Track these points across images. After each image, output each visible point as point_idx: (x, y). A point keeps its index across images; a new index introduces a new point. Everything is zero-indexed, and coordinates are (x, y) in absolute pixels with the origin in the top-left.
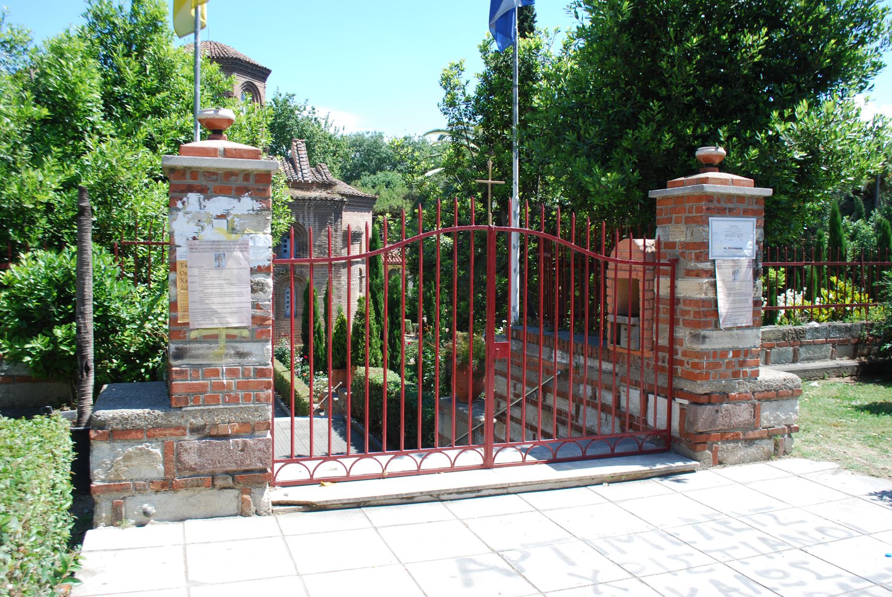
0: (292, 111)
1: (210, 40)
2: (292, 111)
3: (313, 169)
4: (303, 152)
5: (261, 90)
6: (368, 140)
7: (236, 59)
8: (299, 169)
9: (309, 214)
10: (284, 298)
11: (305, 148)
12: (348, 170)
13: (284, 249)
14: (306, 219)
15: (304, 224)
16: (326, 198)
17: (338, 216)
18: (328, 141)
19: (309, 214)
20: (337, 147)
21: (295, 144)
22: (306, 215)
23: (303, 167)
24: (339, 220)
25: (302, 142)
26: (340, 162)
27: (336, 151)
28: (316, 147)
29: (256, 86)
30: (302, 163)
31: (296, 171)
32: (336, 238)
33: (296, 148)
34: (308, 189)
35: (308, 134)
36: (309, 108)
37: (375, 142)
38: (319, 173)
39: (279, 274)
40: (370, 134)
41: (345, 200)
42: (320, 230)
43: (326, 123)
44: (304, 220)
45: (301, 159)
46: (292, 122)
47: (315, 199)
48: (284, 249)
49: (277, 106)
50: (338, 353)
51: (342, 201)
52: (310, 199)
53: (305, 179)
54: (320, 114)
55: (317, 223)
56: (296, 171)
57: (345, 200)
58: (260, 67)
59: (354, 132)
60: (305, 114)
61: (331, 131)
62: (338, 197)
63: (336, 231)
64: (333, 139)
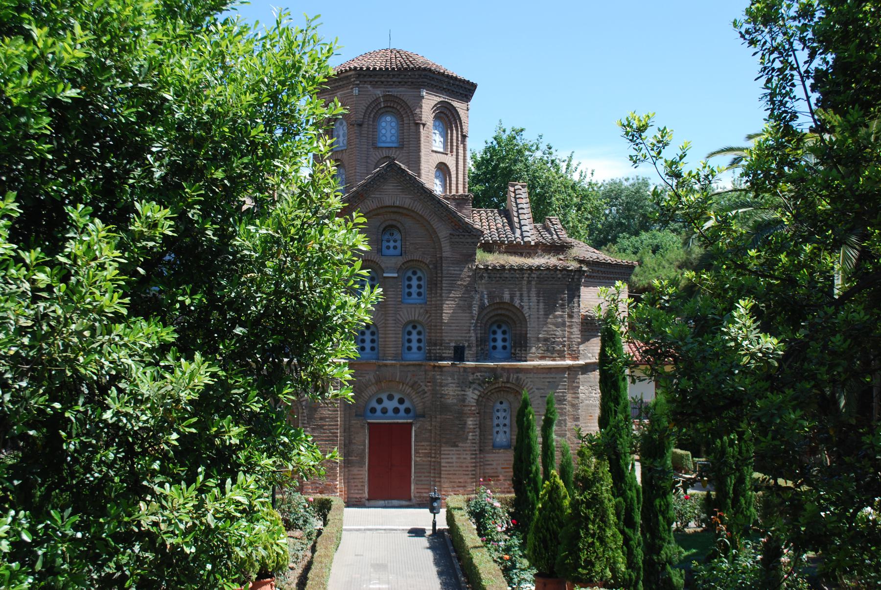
0: (520, 152)
2: (520, 152)
3: (538, 225)
4: (524, 201)
5: (462, 113)
6: (627, 189)
7: (425, 69)
8: (517, 225)
9: (529, 291)
10: (491, 419)
11: (526, 195)
12: (600, 231)
13: (492, 344)
14: (525, 299)
15: (522, 307)
16: (555, 266)
17: (574, 294)
18: (570, 191)
19: (529, 291)
20: (582, 199)
21: (512, 189)
23: (523, 222)
24: (576, 300)
26: (587, 219)
27: (582, 204)
28: (554, 199)
29: (454, 108)
30: (521, 217)
32: (570, 327)
33: (513, 195)
34: (529, 255)
35: (541, 182)
36: (543, 147)
37: (638, 192)
38: (547, 229)
39: (484, 382)
40: (631, 181)
41: (585, 268)
42: (547, 315)
43: (568, 166)
44: (522, 300)
45: (520, 211)
46: (520, 166)
47: (538, 268)
48: (492, 344)
49: (500, 146)
50: (546, 548)
51: (579, 271)
52: (530, 268)
53: (526, 239)
54: (560, 155)
55: (541, 305)
57: (585, 268)
58: (460, 80)
59: (608, 180)
60: (538, 154)
61: (576, 177)
62: (573, 265)
63: (571, 316)
64: (577, 188)
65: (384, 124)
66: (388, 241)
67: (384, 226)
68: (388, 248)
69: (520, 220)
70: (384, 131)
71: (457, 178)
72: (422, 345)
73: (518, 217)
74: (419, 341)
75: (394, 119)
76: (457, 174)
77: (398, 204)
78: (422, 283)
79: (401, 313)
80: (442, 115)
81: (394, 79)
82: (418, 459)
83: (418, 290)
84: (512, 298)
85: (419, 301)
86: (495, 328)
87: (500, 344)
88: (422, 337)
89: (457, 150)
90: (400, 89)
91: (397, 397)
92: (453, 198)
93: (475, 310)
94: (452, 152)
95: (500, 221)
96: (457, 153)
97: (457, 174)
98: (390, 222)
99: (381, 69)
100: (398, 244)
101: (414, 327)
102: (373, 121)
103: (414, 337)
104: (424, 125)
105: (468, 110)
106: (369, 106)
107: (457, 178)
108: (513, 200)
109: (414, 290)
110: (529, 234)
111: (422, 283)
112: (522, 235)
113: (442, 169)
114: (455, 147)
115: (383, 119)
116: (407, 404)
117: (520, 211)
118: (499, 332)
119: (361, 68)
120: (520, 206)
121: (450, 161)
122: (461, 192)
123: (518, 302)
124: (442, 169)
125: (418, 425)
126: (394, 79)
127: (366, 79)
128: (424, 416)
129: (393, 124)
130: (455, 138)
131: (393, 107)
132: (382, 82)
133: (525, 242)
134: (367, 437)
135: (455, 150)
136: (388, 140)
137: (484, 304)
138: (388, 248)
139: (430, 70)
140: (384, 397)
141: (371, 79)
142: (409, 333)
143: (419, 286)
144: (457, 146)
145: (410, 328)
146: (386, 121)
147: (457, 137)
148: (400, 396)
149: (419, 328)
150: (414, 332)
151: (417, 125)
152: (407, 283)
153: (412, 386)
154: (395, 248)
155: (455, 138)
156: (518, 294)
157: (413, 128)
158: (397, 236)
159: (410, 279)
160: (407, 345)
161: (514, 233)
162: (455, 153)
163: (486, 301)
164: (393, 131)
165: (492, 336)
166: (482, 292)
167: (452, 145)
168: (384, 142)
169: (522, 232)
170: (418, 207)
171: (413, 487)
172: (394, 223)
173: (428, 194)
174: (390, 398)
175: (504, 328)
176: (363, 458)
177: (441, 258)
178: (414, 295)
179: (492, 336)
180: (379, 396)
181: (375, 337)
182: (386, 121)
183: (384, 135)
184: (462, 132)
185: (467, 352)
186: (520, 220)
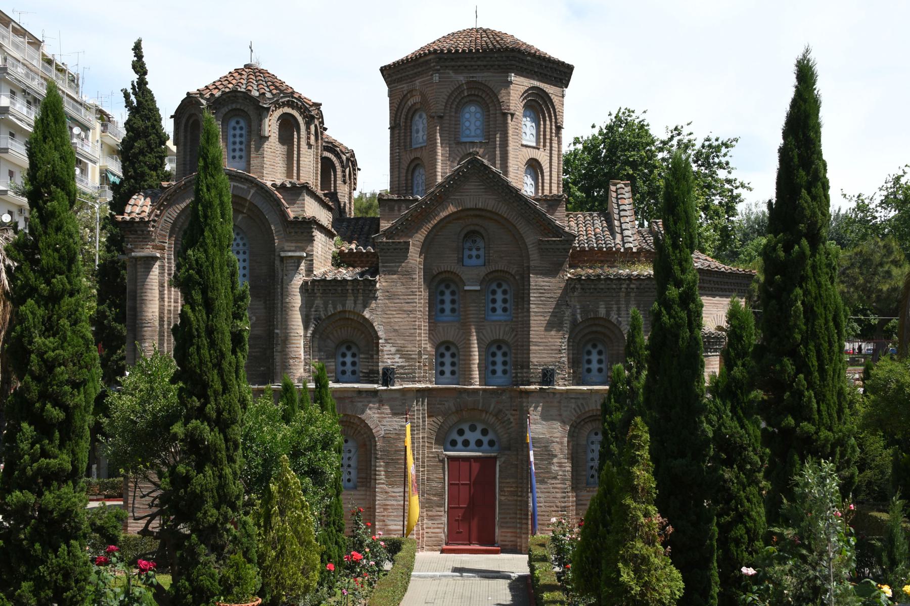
1: (478, 27)
4: (627, 201)
5: (555, 100)
7: (513, 50)
8: (618, 230)
13: (587, 366)
15: (620, 323)
22: (623, 307)
23: (624, 226)
25: (625, 185)
29: (547, 94)
31: (613, 233)
33: (614, 195)
44: (619, 315)
45: (622, 213)
48: (587, 366)
53: (627, 245)
56: (613, 233)
65: (467, 116)
66: (470, 250)
68: (470, 257)
69: (621, 223)
70: (467, 124)
71: (551, 176)
72: (507, 368)
73: (619, 220)
74: (505, 363)
75: (479, 110)
76: (551, 171)
78: (508, 297)
79: (484, 332)
80: (533, 103)
81: (479, 63)
82: (503, 498)
83: (504, 305)
84: (608, 313)
85: (502, 318)
87: (595, 366)
88: (507, 359)
89: (551, 143)
90: (486, 74)
91: (480, 427)
92: (545, 200)
94: (544, 146)
95: (599, 224)
96: (551, 147)
97: (551, 171)
99: (464, 51)
100: (481, 252)
101: (499, 348)
102: (456, 113)
103: (499, 359)
104: (512, 115)
105: (563, 96)
106: (451, 94)
107: (551, 176)
108: (614, 200)
109: (499, 305)
110: (631, 239)
111: (508, 297)
112: (623, 240)
113: (534, 167)
114: (548, 141)
115: (467, 110)
116: (491, 436)
117: (622, 213)
119: (442, 51)
120: (622, 207)
121: (542, 156)
122: (555, 191)
123: (616, 316)
124: (534, 167)
125: (503, 459)
126: (479, 63)
127: (447, 64)
128: (509, 449)
129: (478, 115)
130: (548, 130)
131: (478, 96)
132: (466, 67)
133: (625, 249)
134: (447, 473)
135: (548, 144)
136: (473, 134)
138: (470, 257)
139: (519, 51)
140: (466, 427)
141: (453, 63)
142: (494, 355)
143: (505, 301)
144: (551, 140)
145: (494, 349)
146: (470, 112)
147: (551, 129)
148: (484, 427)
149: (505, 349)
150: (499, 354)
151: (505, 115)
152: (491, 297)
153: (496, 415)
154: (478, 257)
155: (548, 130)
156: (615, 307)
157: (500, 119)
158: (481, 244)
159: (494, 292)
160: (491, 368)
161: (614, 239)
162: (548, 148)
163: (579, 316)
164: (478, 123)
165: (586, 357)
166: (575, 306)
167: (545, 139)
168: (468, 136)
169: (623, 237)
171: (497, 530)
173: (514, 194)
174: (473, 428)
175: (600, 347)
176: (441, 495)
177: (528, 267)
178: (499, 311)
179: (586, 357)
180: (460, 427)
181: (455, 360)
182: (470, 112)
183: (468, 128)
184: (556, 123)
186: (621, 223)
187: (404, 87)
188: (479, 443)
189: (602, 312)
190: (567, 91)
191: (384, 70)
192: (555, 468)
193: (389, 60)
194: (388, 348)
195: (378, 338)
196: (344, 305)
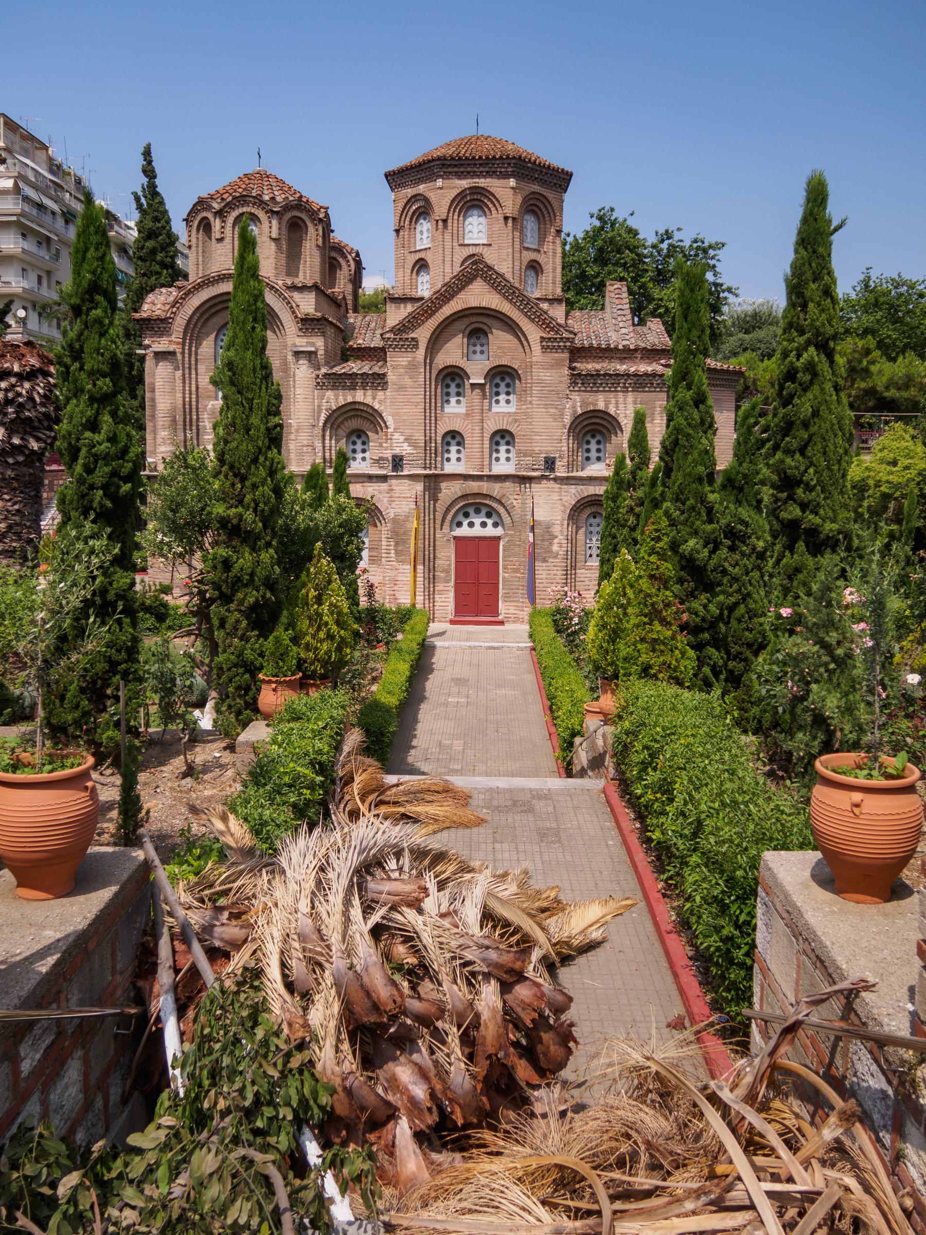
5: (555, 205)
14: (621, 406)
44: (617, 407)
67: (469, 329)
77: (484, 304)
84: (607, 406)
86: (497, 380)
93: (568, 420)
98: (477, 325)
118: (593, 442)
126: (481, 169)
132: (469, 172)
137: (575, 411)
141: (456, 169)
156: (613, 401)
170: (506, 308)
172: (481, 326)
174: (478, 511)
178: (503, 403)
185: (558, 464)
187: (410, 192)
188: (484, 525)
189: (601, 406)
190: (567, 196)
191: (387, 175)
192: (555, 548)
193: (394, 166)
194: (397, 436)
195: (387, 427)
196: (354, 397)
